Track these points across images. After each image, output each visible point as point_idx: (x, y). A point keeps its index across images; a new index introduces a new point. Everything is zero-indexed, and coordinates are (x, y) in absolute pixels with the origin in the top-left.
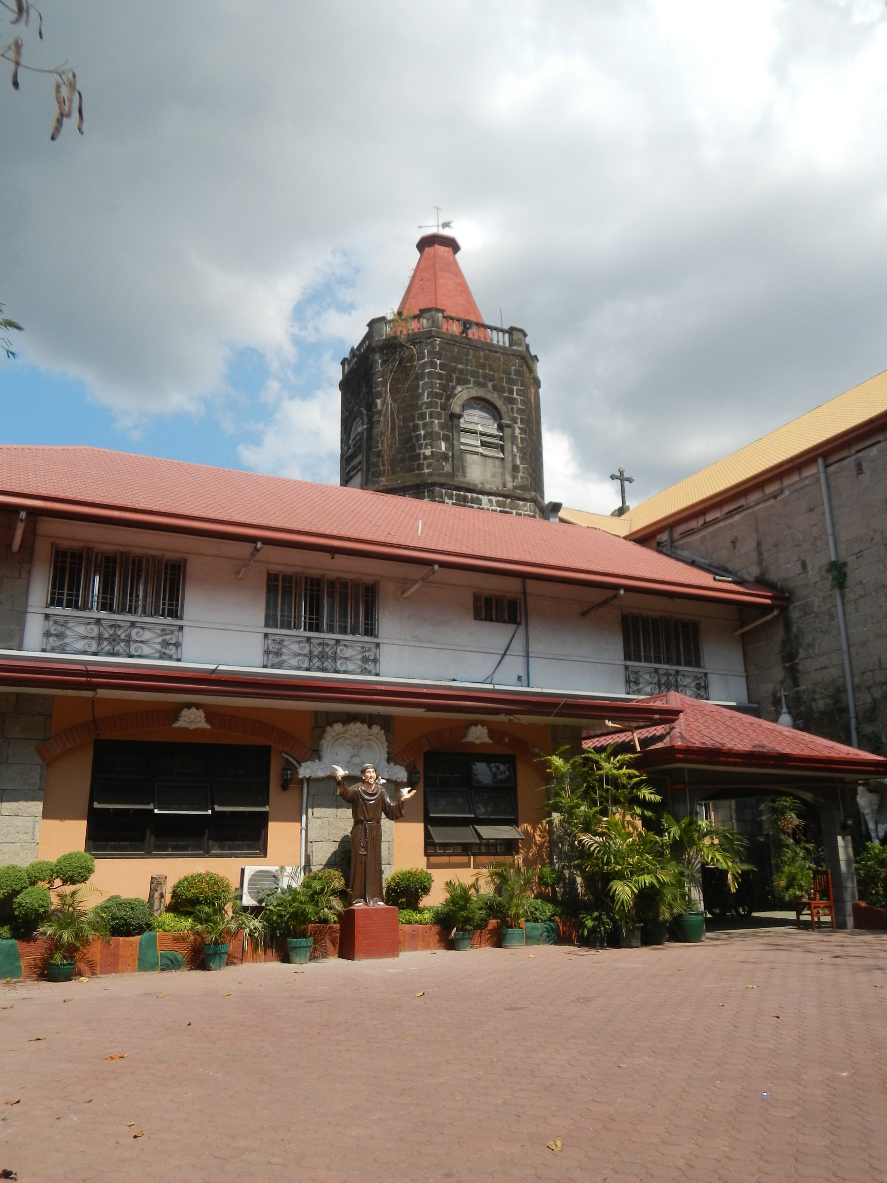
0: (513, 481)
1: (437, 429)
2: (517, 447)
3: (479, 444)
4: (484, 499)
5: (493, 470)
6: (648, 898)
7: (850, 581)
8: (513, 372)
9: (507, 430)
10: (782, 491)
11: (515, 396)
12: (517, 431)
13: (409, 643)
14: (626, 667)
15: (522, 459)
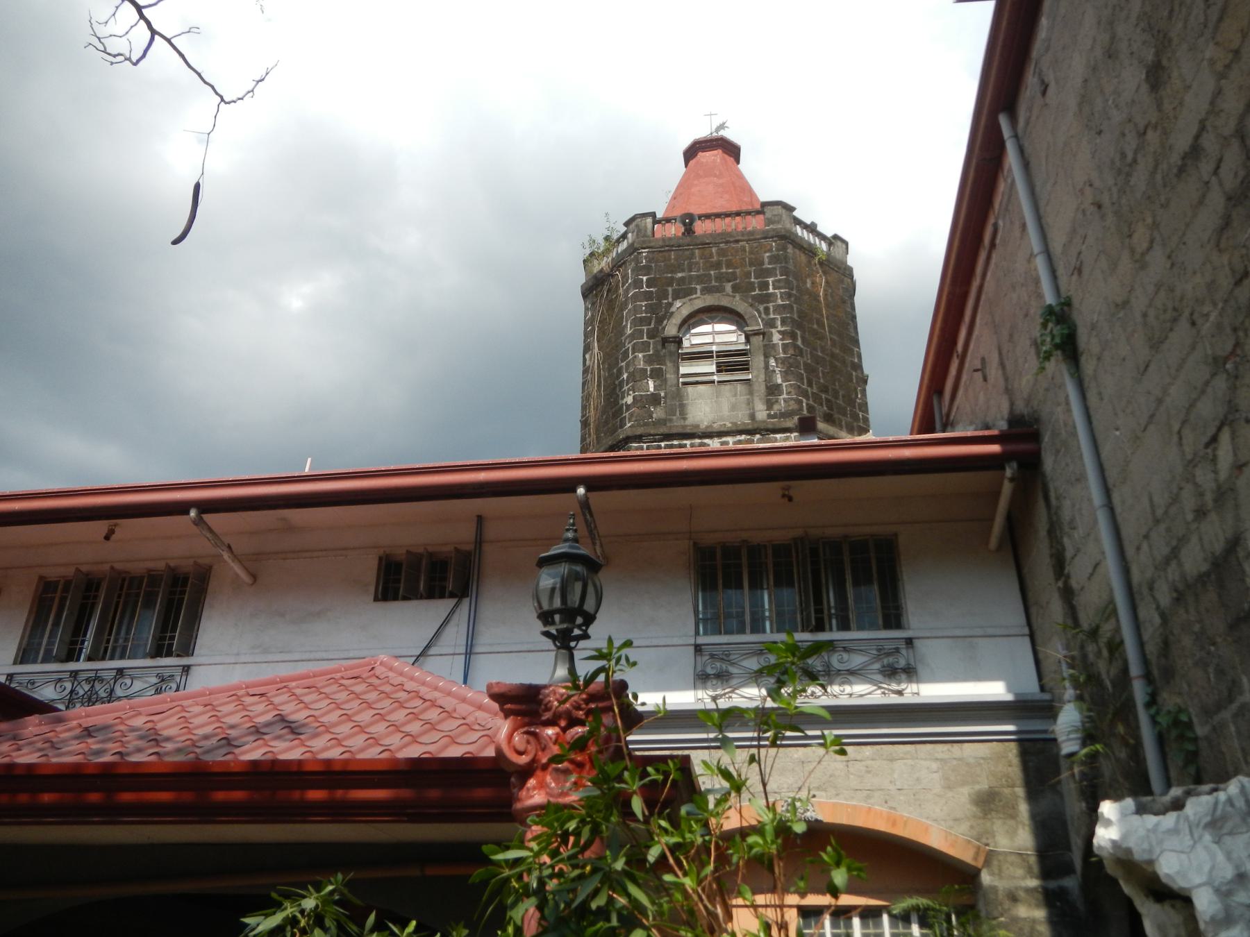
0: (769, 407)
2: (776, 360)
3: (713, 368)
5: (733, 399)
7: (1084, 339)
8: (766, 260)
9: (754, 340)
11: (771, 290)
12: (776, 338)
13: (243, 659)
14: (698, 649)
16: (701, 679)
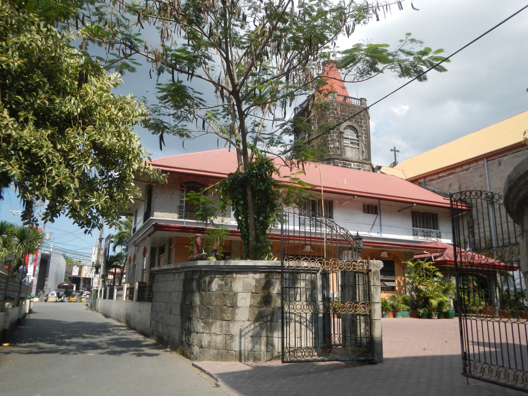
1: (335, 138)
4: (352, 164)
6: (441, 304)
10: (469, 168)
12: (364, 138)
14: (413, 230)
15: (365, 148)
16: (414, 235)
